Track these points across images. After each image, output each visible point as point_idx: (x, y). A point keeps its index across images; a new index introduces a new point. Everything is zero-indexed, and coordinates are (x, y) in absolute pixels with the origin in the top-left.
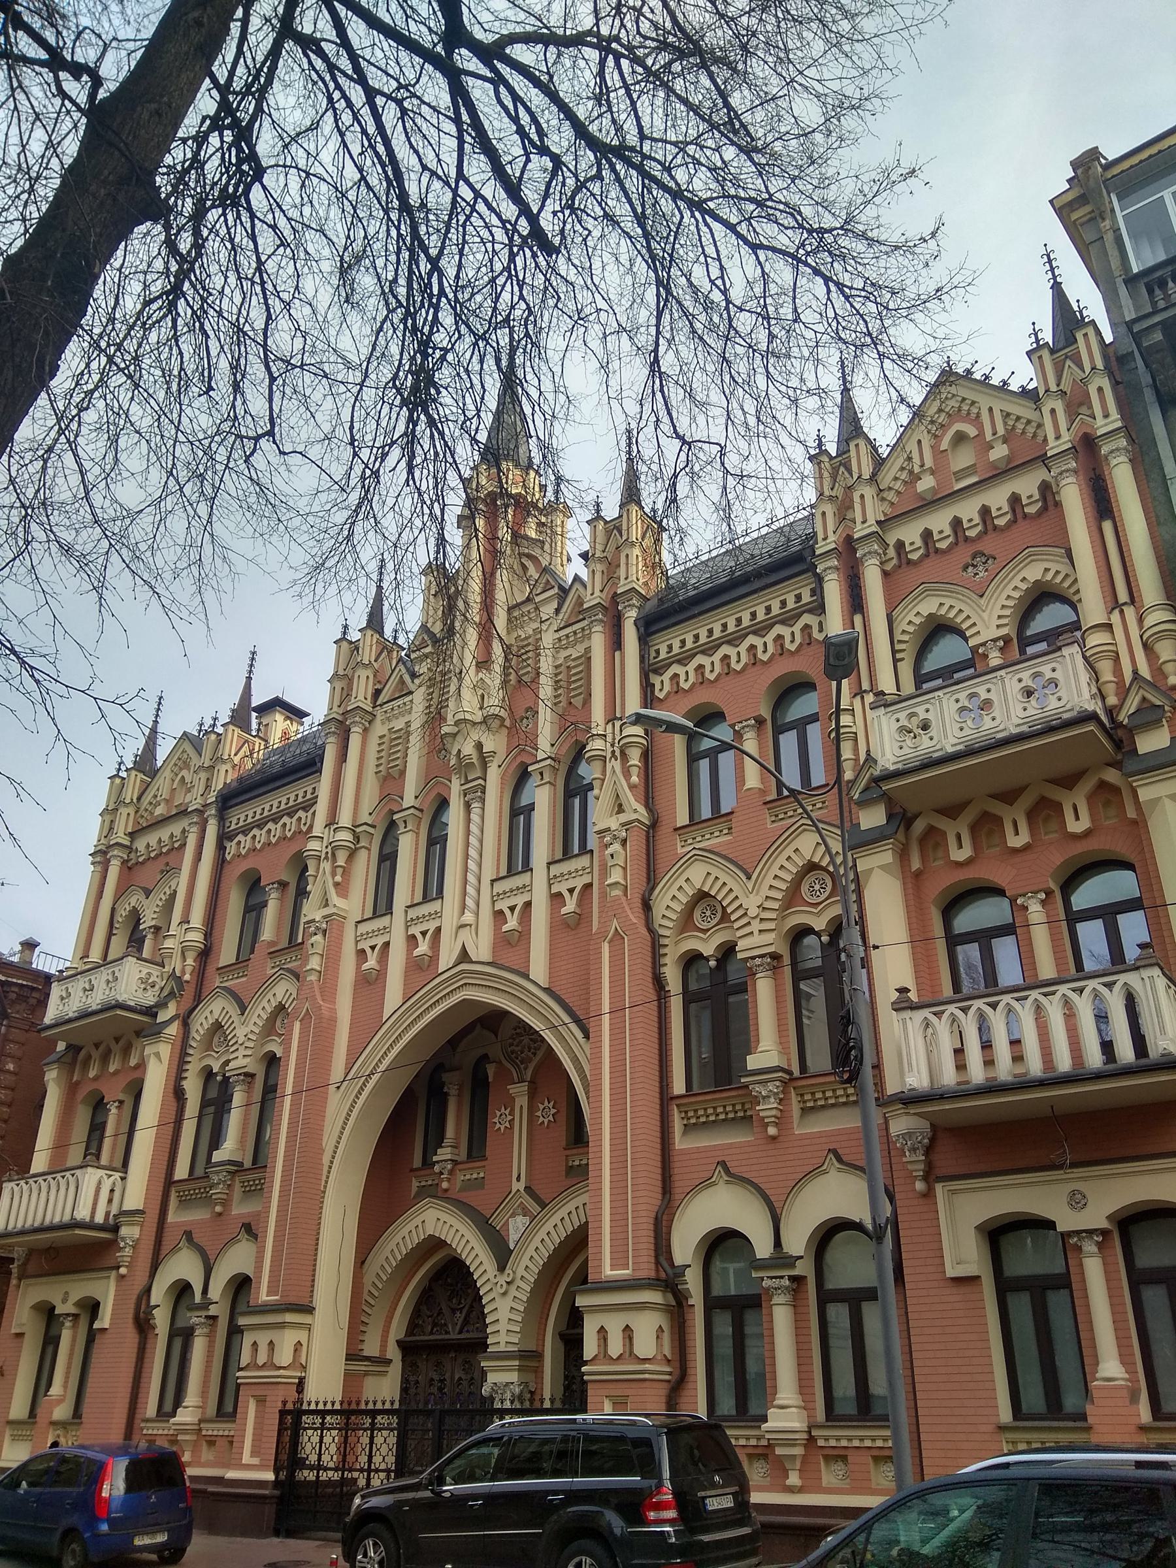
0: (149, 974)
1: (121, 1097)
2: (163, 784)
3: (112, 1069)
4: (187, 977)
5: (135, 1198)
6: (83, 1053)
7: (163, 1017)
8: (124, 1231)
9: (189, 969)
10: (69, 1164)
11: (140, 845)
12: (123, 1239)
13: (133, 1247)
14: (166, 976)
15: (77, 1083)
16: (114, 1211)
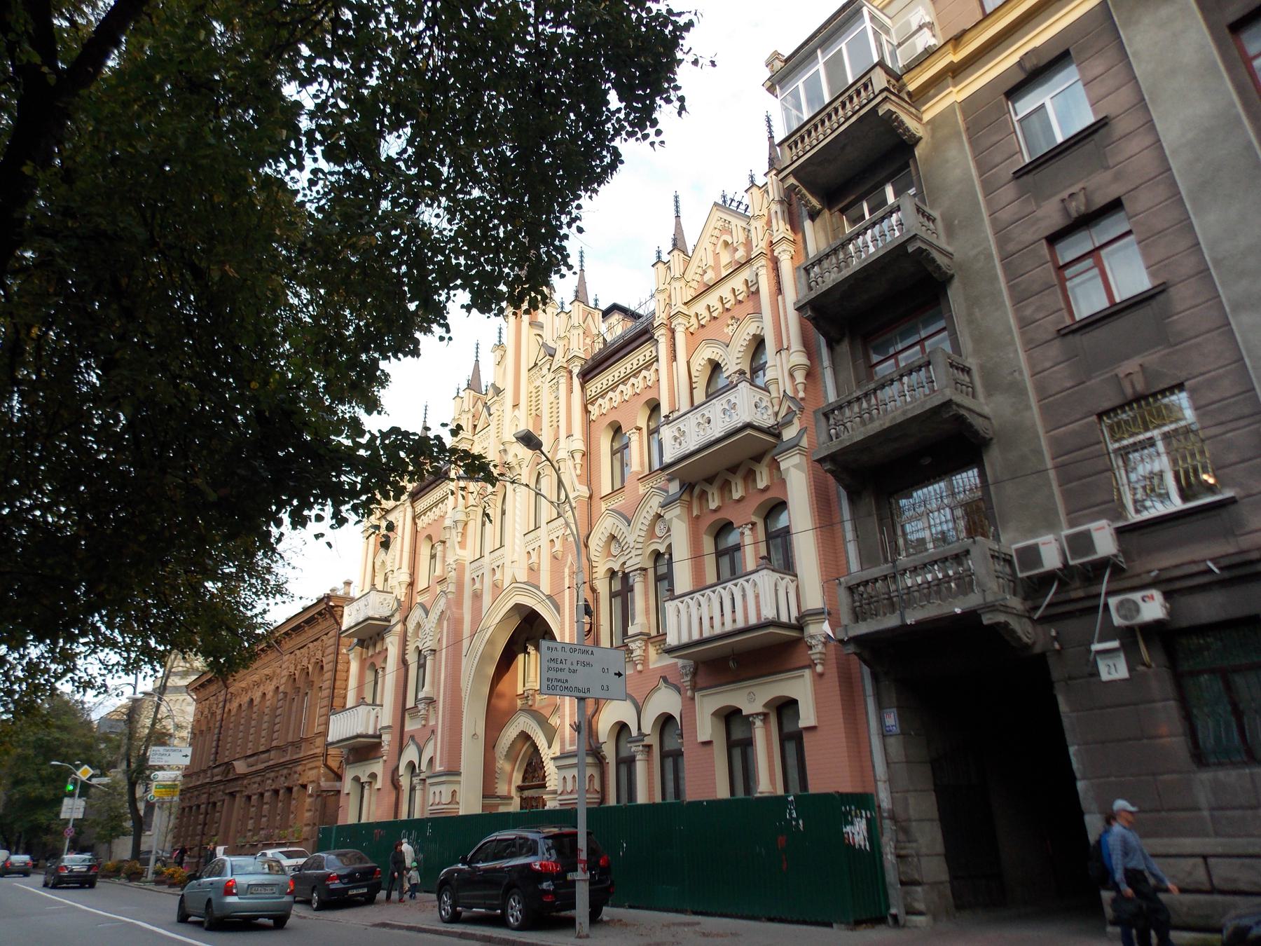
0: (761, 399)
1: (754, 519)
2: (704, 256)
3: (736, 496)
4: (801, 394)
5: (814, 599)
6: (697, 490)
7: (789, 434)
8: (812, 629)
9: (800, 387)
10: (709, 582)
11: (700, 307)
12: (812, 637)
13: (825, 644)
14: (776, 401)
15: (698, 517)
16: (794, 613)
